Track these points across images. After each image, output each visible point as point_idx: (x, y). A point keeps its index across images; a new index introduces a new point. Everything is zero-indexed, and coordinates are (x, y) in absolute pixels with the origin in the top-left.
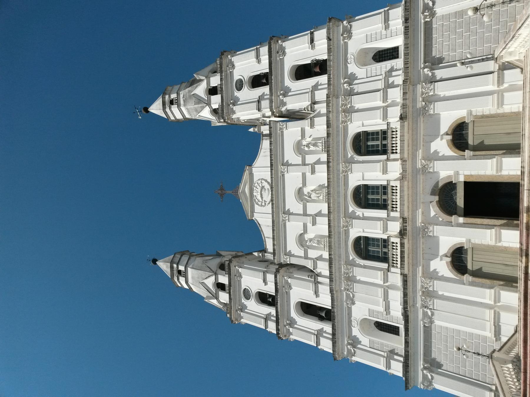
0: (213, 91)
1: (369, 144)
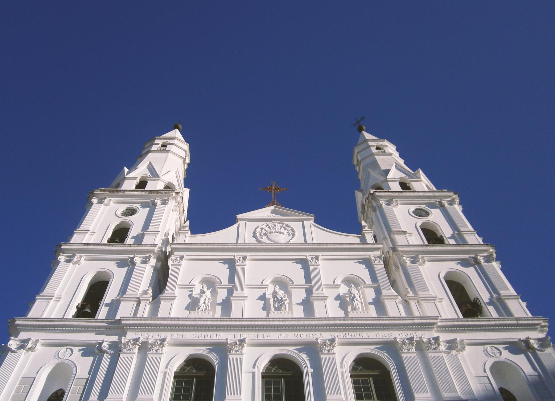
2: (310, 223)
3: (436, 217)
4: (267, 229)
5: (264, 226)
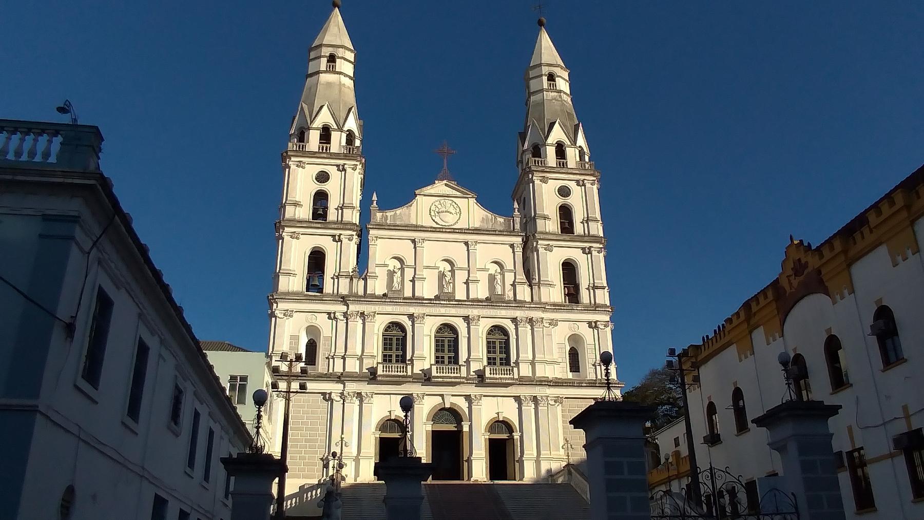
0: (560, 151)
1: (500, 345)
2: (472, 201)
3: (576, 201)
4: (439, 206)
5: (437, 204)
